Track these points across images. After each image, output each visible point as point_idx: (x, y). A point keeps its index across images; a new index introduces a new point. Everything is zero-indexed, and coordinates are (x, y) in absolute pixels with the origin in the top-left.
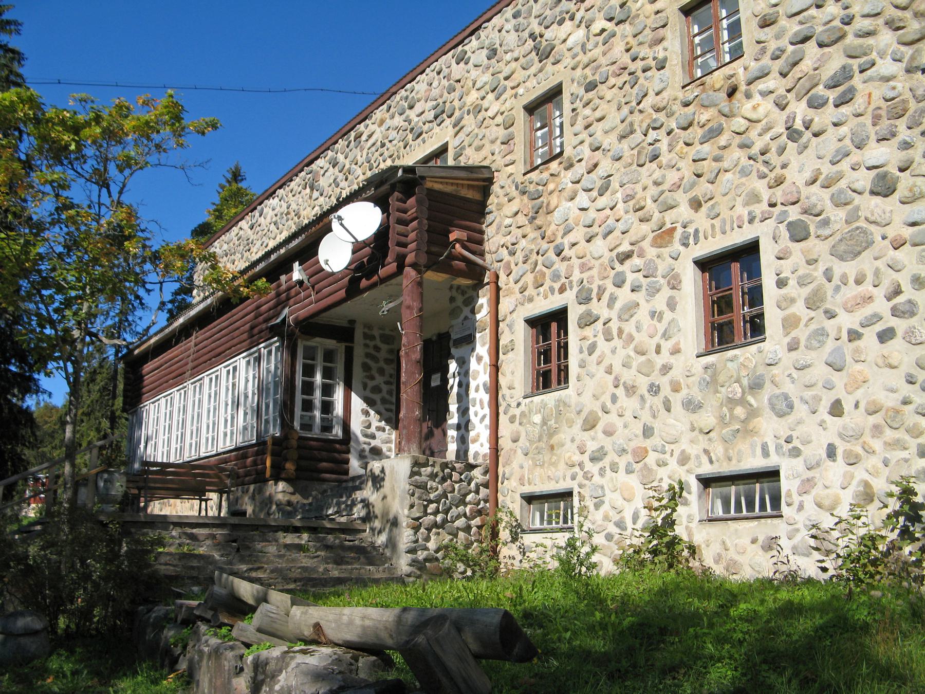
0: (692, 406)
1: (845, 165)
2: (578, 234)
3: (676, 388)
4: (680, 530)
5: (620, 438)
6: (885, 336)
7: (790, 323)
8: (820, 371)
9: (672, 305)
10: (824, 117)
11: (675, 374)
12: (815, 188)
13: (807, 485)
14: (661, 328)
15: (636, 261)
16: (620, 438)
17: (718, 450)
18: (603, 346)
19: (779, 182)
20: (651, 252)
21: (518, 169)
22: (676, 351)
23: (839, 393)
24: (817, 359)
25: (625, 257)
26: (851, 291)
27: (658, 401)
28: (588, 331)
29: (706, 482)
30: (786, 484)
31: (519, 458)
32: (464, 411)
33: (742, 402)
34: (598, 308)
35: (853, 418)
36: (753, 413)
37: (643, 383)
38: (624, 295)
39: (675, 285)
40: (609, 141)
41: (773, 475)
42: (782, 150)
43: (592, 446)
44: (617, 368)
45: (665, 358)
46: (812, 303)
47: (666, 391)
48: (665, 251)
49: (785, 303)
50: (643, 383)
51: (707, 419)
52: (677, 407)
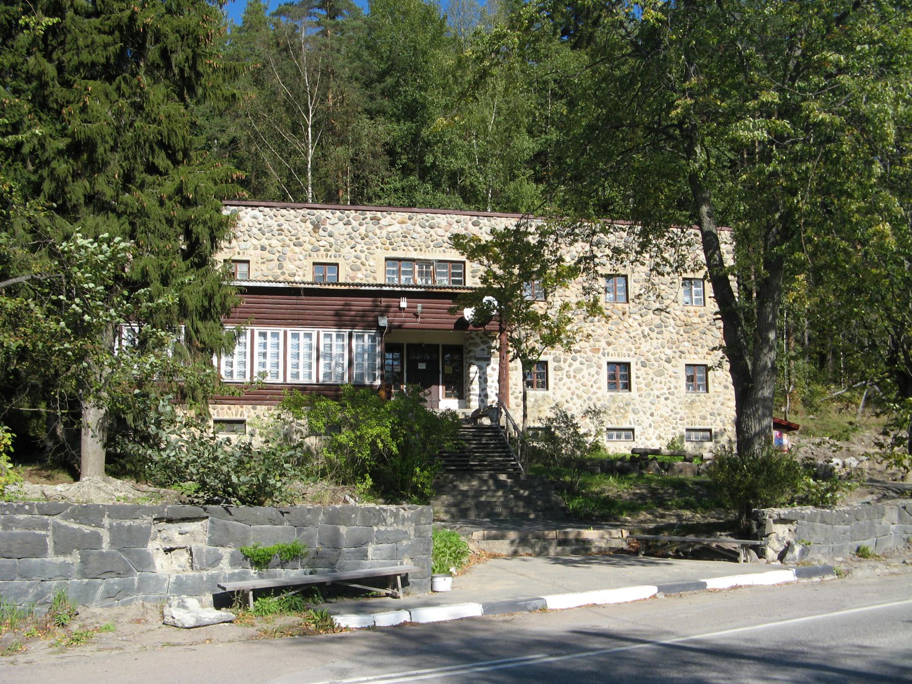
1: (658, 351)
6: (666, 399)
8: (648, 404)
10: (654, 335)
12: (649, 354)
13: (643, 433)
19: (639, 348)
33: (623, 408)
35: (656, 418)
36: (626, 412)
41: (633, 430)
42: (640, 339)
48: (596, 355)
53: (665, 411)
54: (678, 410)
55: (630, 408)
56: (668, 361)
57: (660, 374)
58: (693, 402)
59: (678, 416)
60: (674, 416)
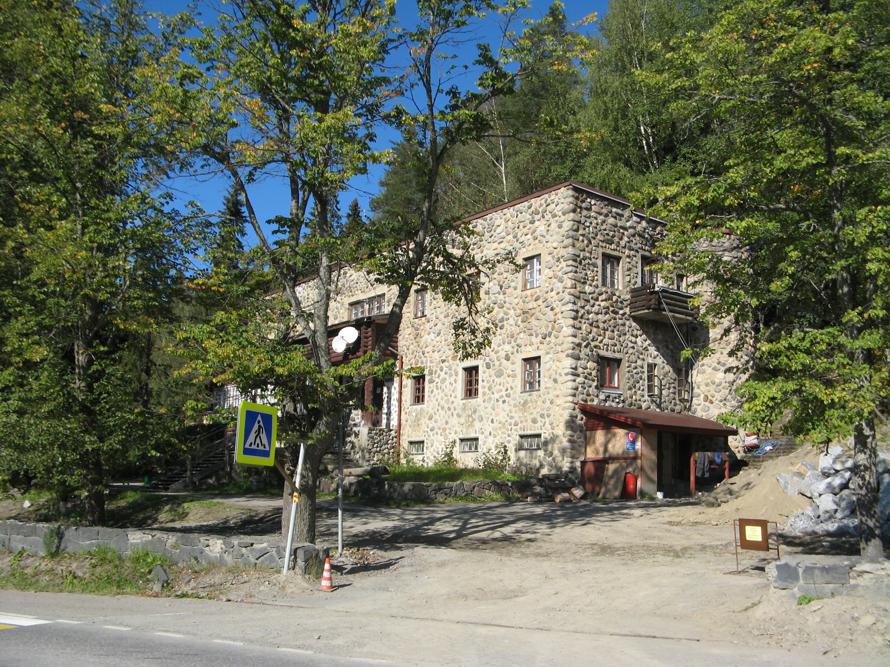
0: (459, 416)
3: (455, 409)
4: (454, 455)
5: (439, 424)
7: (484, 394)
8: (490, 409)
9: (455, 381)
11: (455, 404)
14: (452, 388)
15: (446, 364)
16: (439, 424)
17: (465, 430)
18: (435, 391)
20: (451, 362)
22: (456, 397)
23: (493, 417)
24: (489, 405)
25: (443, 361)
26: (498, 387)
27: (449, 413)
28: (431, 385)
29: (462, 440)
30: (480, 442)
33: (471, 416)
36: (474, 420)
37: (446, 406)
38: (442, 374)
39: (457, 374)
41: (476, 439)
43: (431, 426)
44: (439, 400)
45: (452, 399)
46: (490, 388)
47: (452, 409)
49: (484, 387)
50: (446, 406)
51: (462, 420)
52: (455, 415)
53: (502, 417)
54: (513, 414)
55: (475, 416)
56: (507, 358)
57: (499, 374)
58: (526, 402)
59: (513, 421)
60: (509, 421)
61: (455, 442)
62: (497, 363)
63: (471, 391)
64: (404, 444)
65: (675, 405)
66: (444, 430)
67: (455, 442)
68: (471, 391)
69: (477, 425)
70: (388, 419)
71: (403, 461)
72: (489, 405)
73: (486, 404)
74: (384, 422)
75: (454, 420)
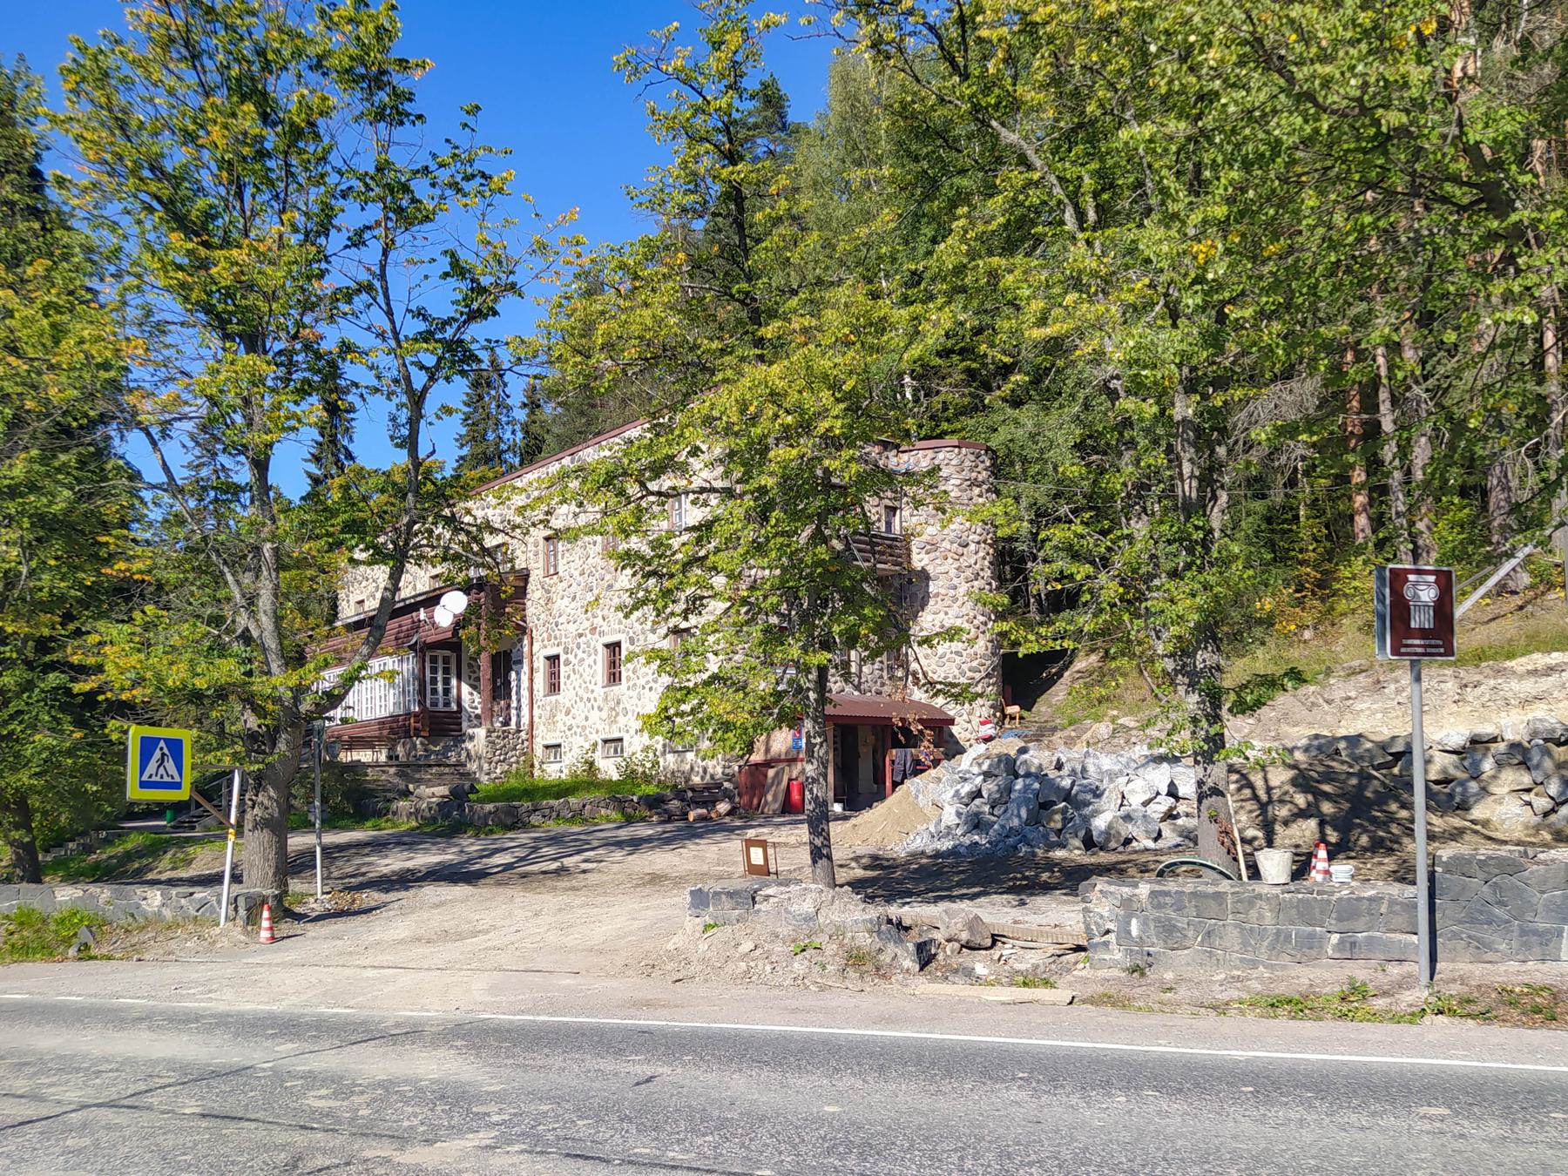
0: (600, 709)
2: (563, 619)
7: (628, 679)
8: (635, 700)
18: (573, 677)
21: (540, 572)
24: (634, 694)
25: (580, 635)
29: (606, 741)
30: (625, 743)
31: (542, 727)
32: (519, 701)
34: (571, 657)
40: (576, 574)
41: (621, 740)
51: (604, 715)
55: (619, 709)
61: (595, 745)
62: (642, 637)
63: (614, 677)
64: (539, 751)
65: (883, 685)
66: (584, 728)
67: (595, 745)
68: (614, 677)
69: (621, 719)
70: (518, 716)
71: (537, 773)
72: (634, 694)
73: (631, 693)
74: (514, 720)
75: (595, 715)
